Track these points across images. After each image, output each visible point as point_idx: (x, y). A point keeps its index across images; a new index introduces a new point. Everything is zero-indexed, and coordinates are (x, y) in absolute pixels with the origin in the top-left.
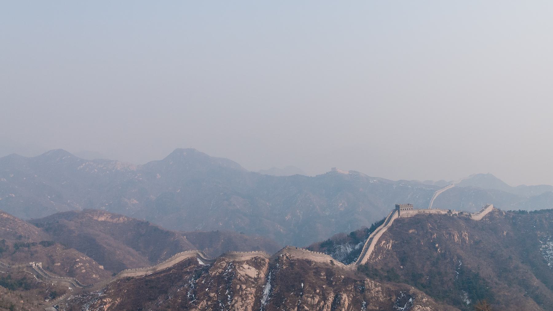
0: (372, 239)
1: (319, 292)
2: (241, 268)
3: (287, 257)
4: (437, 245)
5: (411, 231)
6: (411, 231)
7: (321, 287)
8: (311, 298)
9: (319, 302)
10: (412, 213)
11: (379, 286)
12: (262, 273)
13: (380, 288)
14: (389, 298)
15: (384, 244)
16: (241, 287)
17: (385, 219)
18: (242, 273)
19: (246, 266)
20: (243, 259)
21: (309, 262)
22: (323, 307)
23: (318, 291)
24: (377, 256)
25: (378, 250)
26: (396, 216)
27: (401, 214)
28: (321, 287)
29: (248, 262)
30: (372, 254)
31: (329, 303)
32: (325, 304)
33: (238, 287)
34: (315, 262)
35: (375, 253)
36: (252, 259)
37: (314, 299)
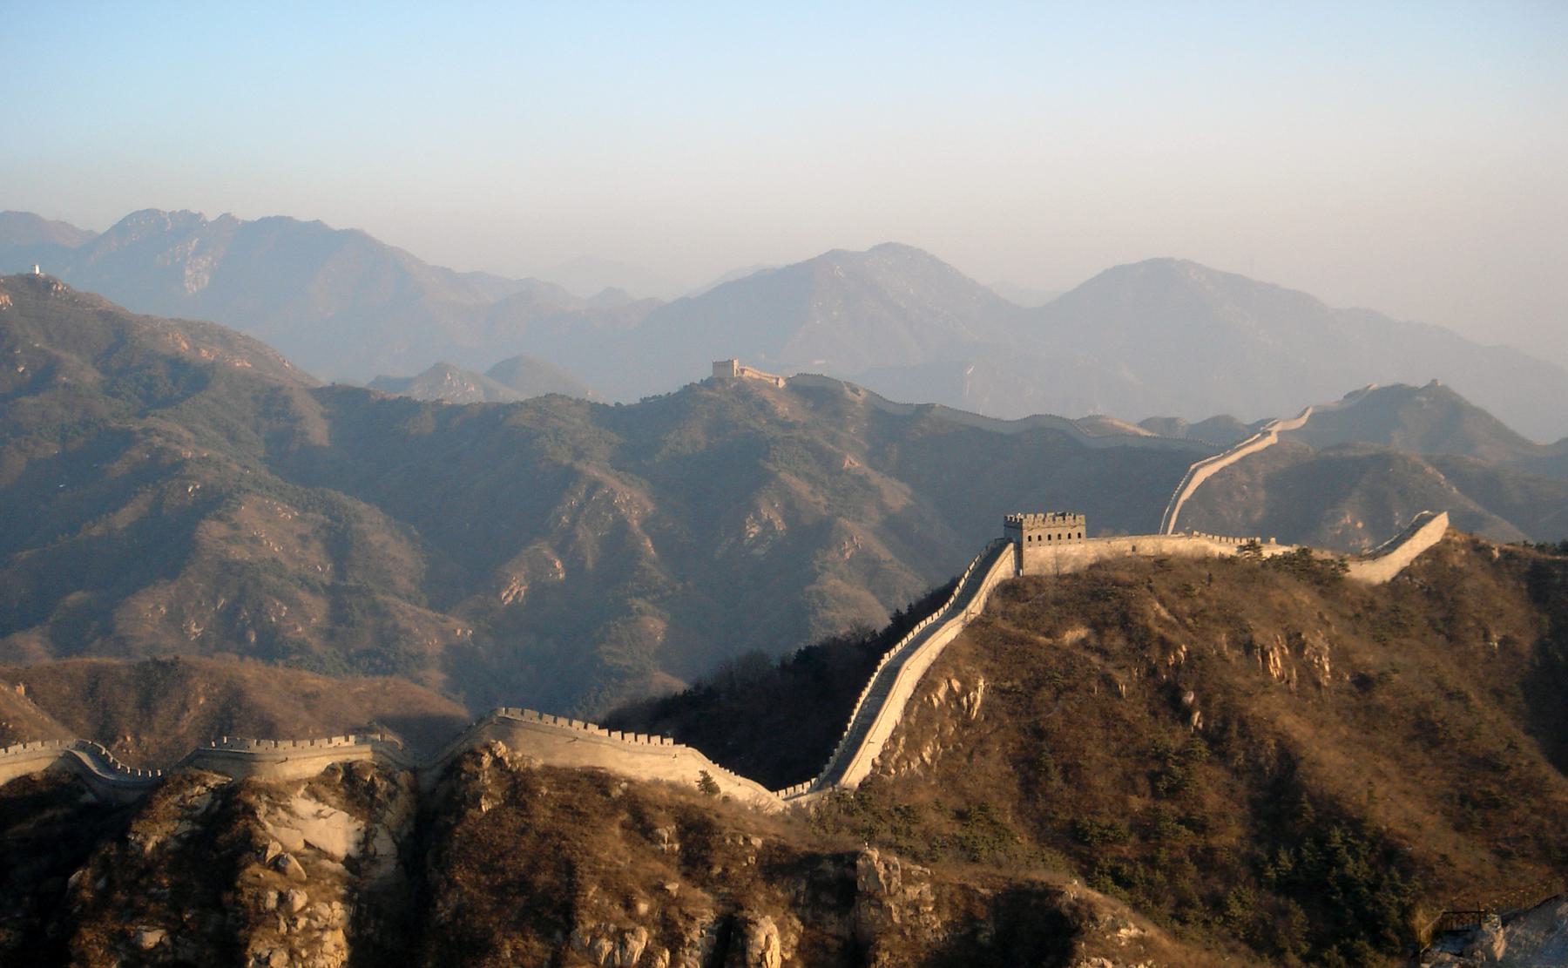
0: (892, 672)
1: (651, 912)
2: (282, 814)
8: (611, 938)
11: (919, 879)
12: (382, 834)
17: (955, 583)
19: (304, 806)
20: (290, 771)
21: (599, 781)
23: (643, 908)
24: (914, 746)
27: (1026, 560)
28: (658, 889)
29: (315, 788)
30: (893, 739)
33: (272, 900)
34: (630, 782)
35: (909, 734)
37: (624, 944)
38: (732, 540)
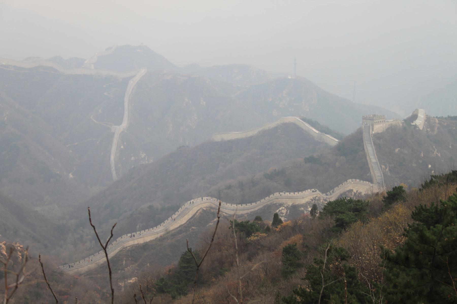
3: (355, 194)
4: (430, 166)
5: (397, 150)
6: (397, 150)
27: (375, 129)
36: (312, 200)
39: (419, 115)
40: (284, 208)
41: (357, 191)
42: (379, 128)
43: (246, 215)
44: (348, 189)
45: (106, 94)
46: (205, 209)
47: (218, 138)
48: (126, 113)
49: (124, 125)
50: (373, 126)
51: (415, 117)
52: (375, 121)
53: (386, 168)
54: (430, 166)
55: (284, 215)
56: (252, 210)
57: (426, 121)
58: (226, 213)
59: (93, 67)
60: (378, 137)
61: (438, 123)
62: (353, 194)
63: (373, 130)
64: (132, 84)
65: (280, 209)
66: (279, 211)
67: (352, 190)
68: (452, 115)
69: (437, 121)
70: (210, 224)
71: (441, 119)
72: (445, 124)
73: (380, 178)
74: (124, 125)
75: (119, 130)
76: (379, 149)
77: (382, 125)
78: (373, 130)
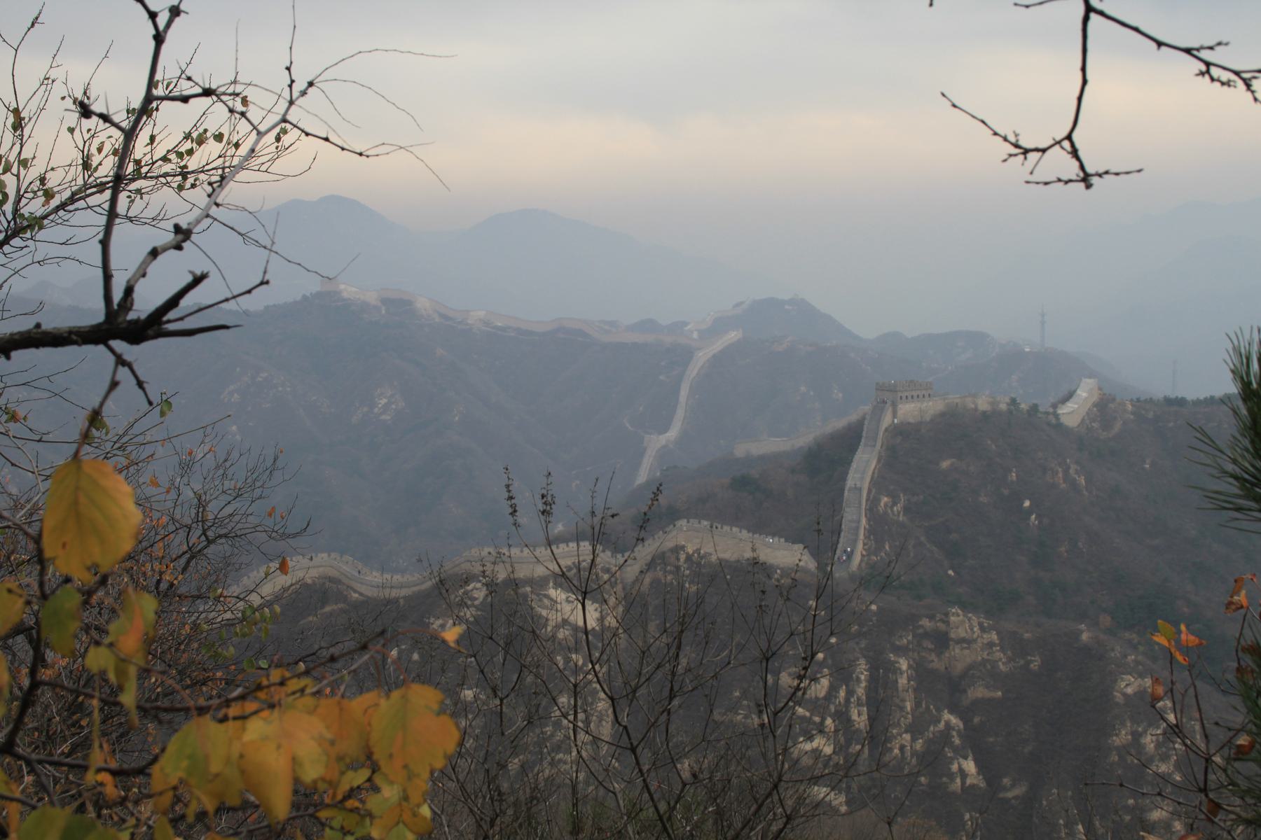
4: (1027, 504)
5: (945, 464)
6: (945, 464)
7: (829, 648)
9: (833, 689)
10: (932, 407)
11: (991, 628)
13: (994, 637)
14: (1022, 662)
15: (886, 505)
16: (567, 660)
18: (554, 618)
22: (847, 700)
25: (879, 527)
26: (887, 420)
27: (900, 413)
29: (562, 578)
31: (860, 691)
32: (850, 693)
34: (782, 569)
38: (365, 409)
39: (1079, 392)
40: (479, 585)
41: (698, 551)
42: (909, 411)
43: (402, 601)
44: (670, 544)
45: (661, 377)
46: (309, 581)
47: (741, 450)
48: (680, 413)
49: (673, 434)
50: (894, 405)
51: (1069, 396)
52: (900, 394)
53: (895, 504)
54: (1027, 504)
55: (476, 603)
56: (415, 589)
57: (1095, 405)
58: (361, 594)
59: (695, 335)
60: (902, 432)
61: (1132, 413)
62: (683, 557)
63: (895, 415)
64: (702, 357)
65: (470, 588)
66: (466, 593)
67: (683, 548)
68: (1173, 396)
69: (1130, 407)
70: (310, 618)
71: (1142, 404)
72: (1151, 415)
73: (854, 525)
74: (673, 434)
75: (656, 442)
76: (891, 460)
77: (919, 405)
78: (895, 415)
